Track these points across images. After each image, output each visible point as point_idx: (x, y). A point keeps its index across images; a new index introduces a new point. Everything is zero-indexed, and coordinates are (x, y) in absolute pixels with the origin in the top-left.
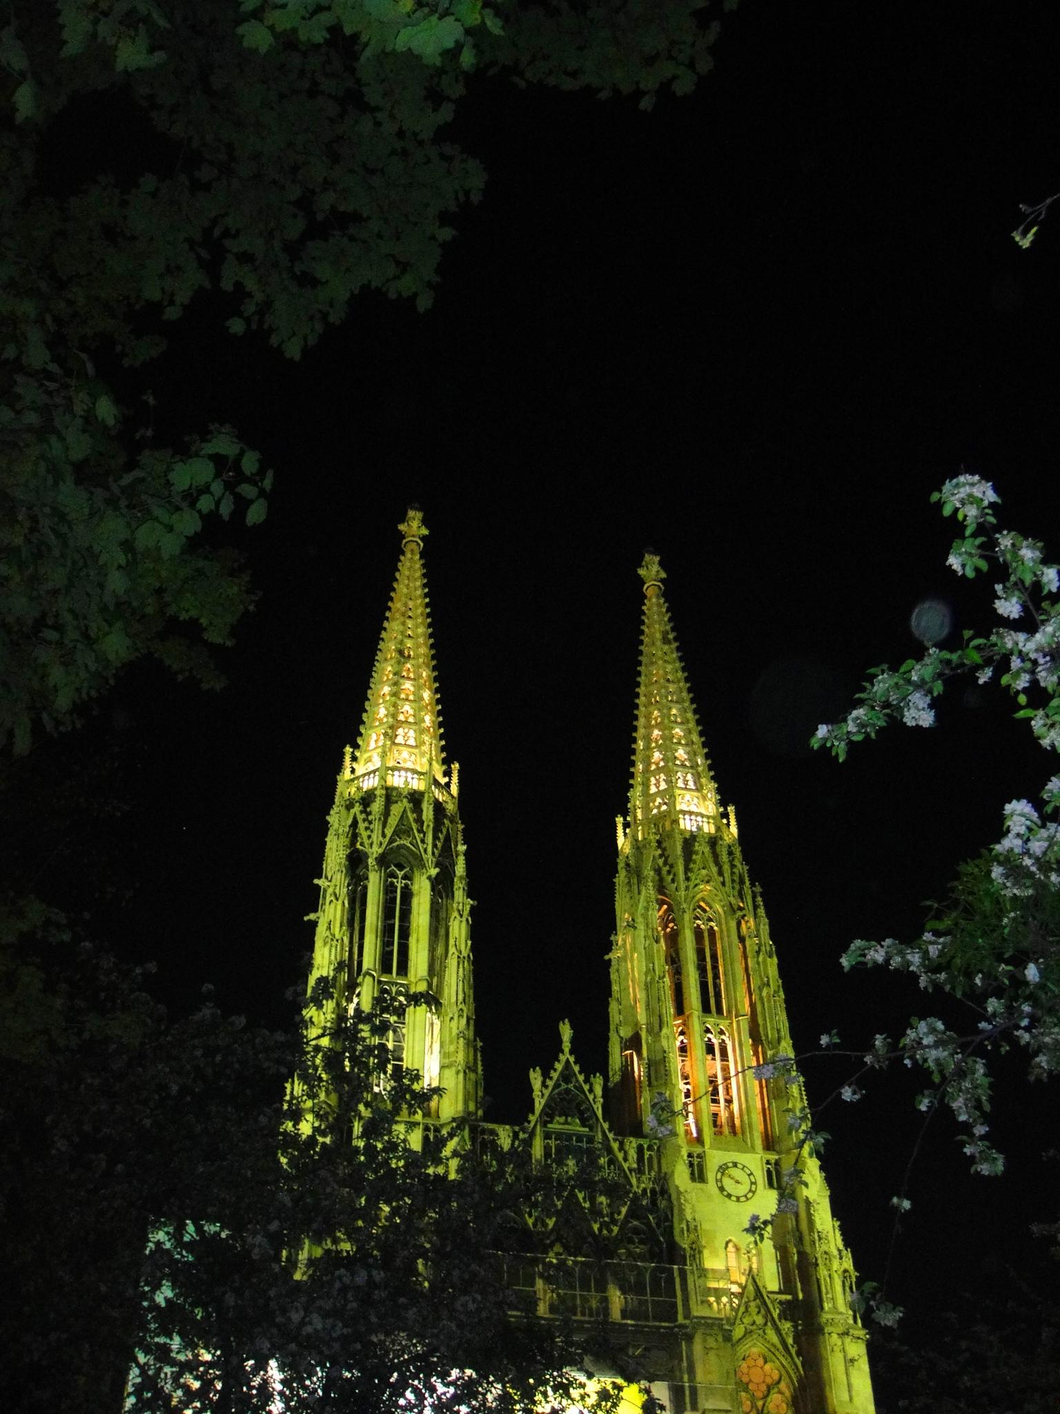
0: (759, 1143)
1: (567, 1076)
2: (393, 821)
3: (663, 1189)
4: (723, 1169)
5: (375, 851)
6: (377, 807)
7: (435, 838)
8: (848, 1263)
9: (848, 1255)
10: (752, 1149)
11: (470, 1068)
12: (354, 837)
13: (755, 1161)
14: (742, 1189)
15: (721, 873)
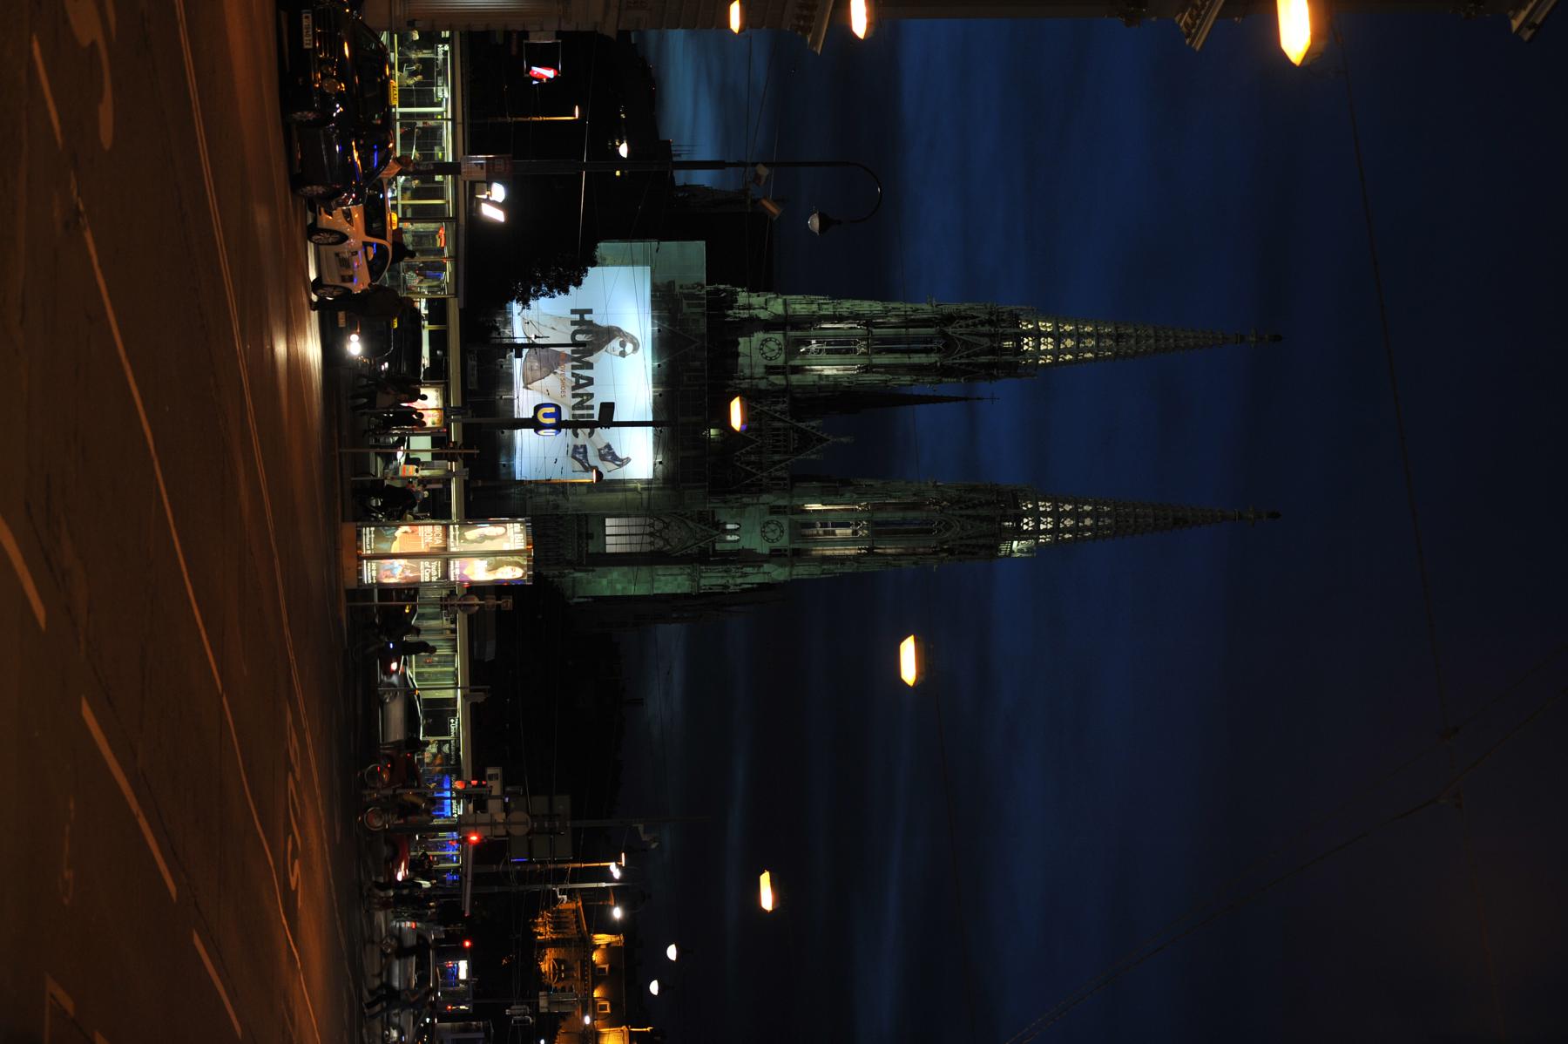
0: (796, 546)
1: (821, 440)
2: (971, 339)
3: (762, 490)
4: (778, 524)
5: (950, 330)
6: (986, 329)
7: (968, 365)
8: (732, 589)
9: (737, 589)
10: (792, 541)
11: (820, 388)
12: (965, 318)
13: (784, 542)
14: (770, 535)
15: (969, 537)
